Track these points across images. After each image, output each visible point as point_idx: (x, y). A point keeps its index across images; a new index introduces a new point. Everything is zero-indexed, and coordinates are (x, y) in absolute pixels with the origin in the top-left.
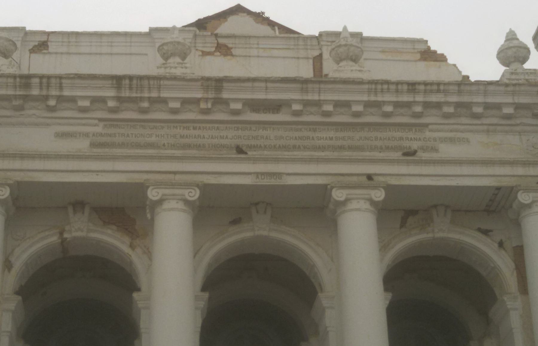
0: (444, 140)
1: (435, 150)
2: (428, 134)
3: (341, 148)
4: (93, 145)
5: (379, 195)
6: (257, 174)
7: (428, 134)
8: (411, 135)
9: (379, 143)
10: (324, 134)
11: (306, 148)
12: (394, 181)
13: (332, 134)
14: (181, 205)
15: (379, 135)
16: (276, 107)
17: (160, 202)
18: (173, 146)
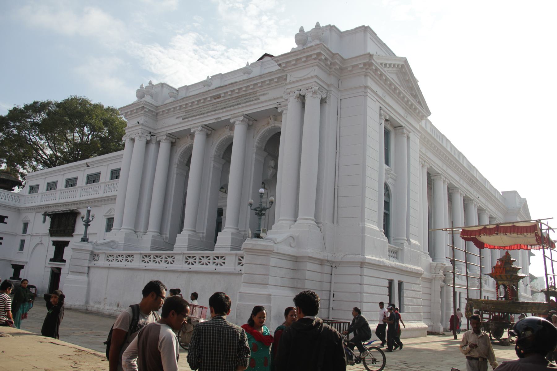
0: (261, 95)
1: (259, 99)
2: (258, 94)
3: (235, 105)
4: (183, 119)
5: (242, 118)
6: (216, 119)
7: (258, 94)
8: (253, 96)
9: (245, 101)
10: (231, 102)
11: (227, 107)
12: (247, 113)
13: (234, 101)
14: (199, 132)
15: (245, 98)
16: (219, 97)
17: (194, 132)
18: (199, 115)
